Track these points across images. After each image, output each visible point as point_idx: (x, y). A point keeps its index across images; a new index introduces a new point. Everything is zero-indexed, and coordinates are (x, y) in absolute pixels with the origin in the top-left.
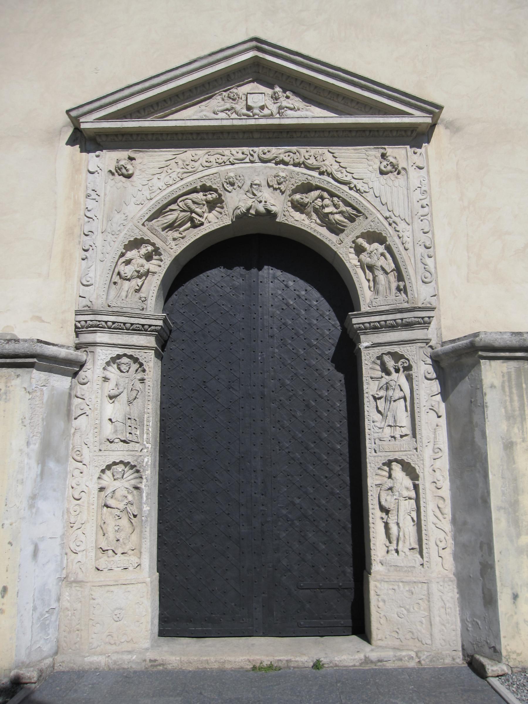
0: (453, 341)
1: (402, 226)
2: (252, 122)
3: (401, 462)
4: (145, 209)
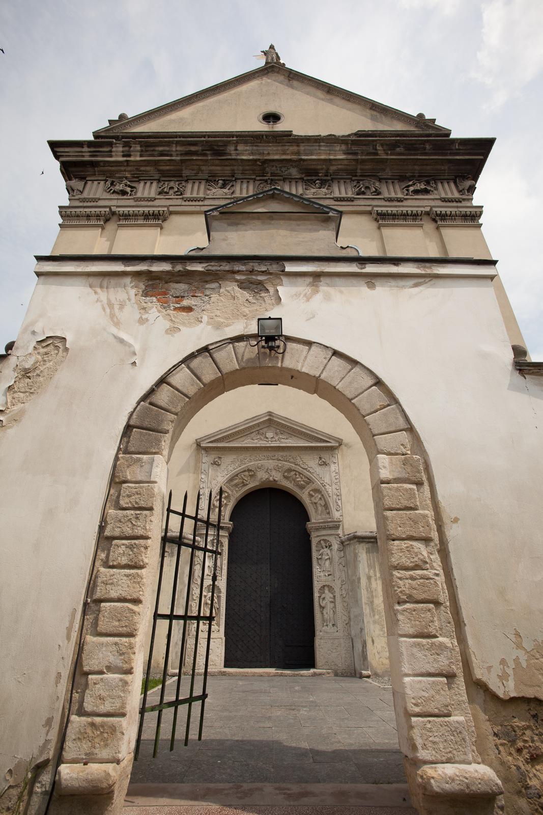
0: (348, 535)
1: (327, 487)
2: (269, 445)
3: (328, 586)
4: (225, 479)
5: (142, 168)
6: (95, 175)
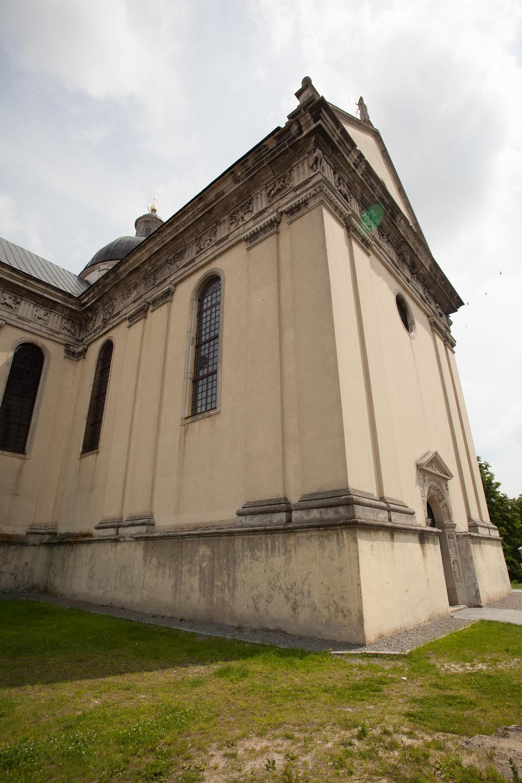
5: (356, 184)
6: (330, 158)
